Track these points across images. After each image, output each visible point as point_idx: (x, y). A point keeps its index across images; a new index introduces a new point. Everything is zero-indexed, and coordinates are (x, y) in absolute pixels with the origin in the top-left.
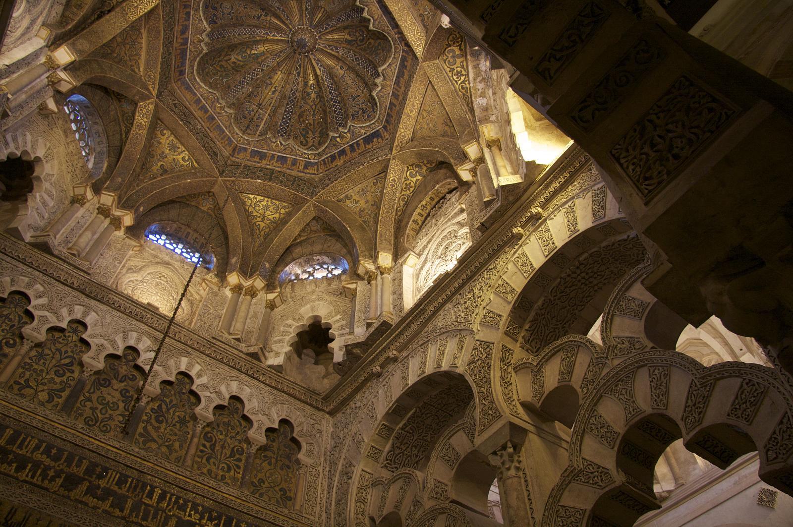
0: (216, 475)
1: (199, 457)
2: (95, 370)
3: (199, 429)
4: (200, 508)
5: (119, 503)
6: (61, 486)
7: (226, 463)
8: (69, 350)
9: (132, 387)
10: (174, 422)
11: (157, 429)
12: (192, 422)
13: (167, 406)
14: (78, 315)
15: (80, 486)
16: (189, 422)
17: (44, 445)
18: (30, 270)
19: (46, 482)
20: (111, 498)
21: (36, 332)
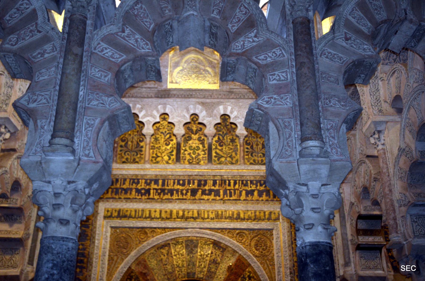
0: (258, 161)
1: (247, 155)
2: (182, 135)
3: (242, 140)
4: (255, 182)
5: (217, 193)
6: (191, 195)
7: (261, 153)
8: (166, 130)
9: (202, 135)
10: (228, 143)
11: (221, 150)
12: (237, 139)
13: (222, 136)
14: (162, 111)
16: (235, 139)
17: (176, 181)
18: (130, 99)
20: (213, 193)
21: (148, 130)
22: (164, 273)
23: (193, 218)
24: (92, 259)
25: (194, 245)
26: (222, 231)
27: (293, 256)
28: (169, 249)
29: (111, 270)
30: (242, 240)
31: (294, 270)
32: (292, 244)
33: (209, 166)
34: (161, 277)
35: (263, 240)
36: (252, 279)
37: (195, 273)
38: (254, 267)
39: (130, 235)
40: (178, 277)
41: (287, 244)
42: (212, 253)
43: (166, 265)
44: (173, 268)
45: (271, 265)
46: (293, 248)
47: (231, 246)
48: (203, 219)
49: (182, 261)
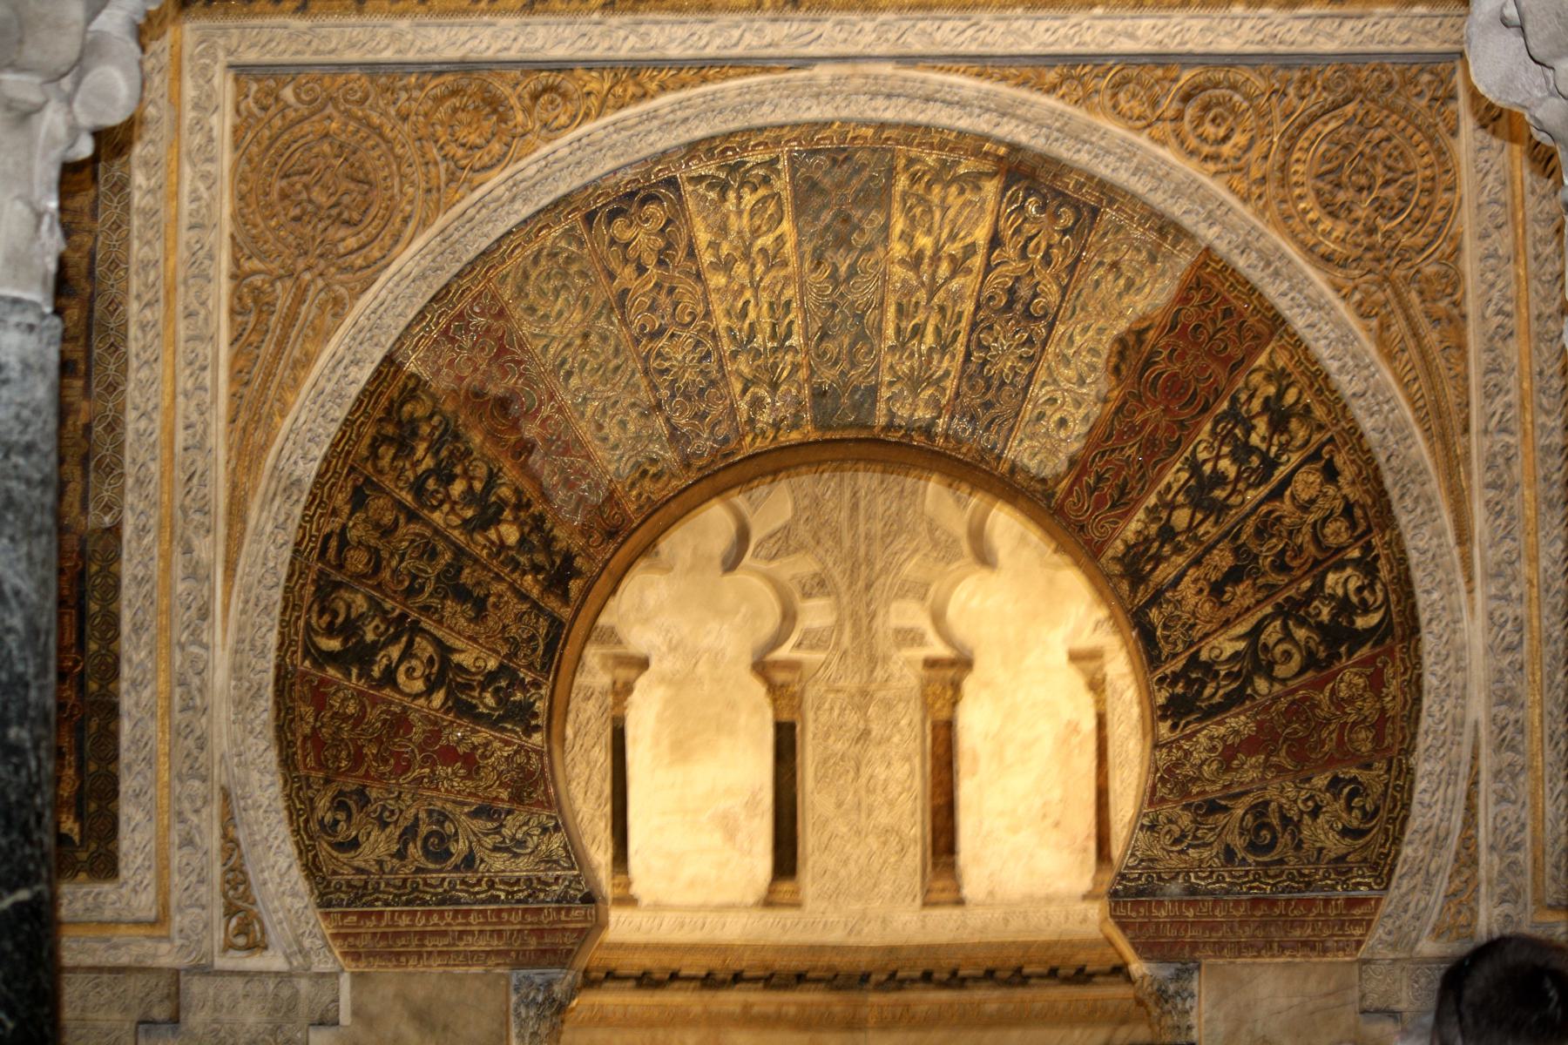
22: (645, 395)
24: (115, 306)
25: (855, 183)
28: (669, 222)
34: (623, 424)
35: (1379, 133)
36: (1294, 424)
37: (873, 391)
39: (376, 119)
40: (751, 421)
42: (995, 241)
43: (656, 334)
44: (708, 355)
47: (1139, 185)
49: (771, 304)
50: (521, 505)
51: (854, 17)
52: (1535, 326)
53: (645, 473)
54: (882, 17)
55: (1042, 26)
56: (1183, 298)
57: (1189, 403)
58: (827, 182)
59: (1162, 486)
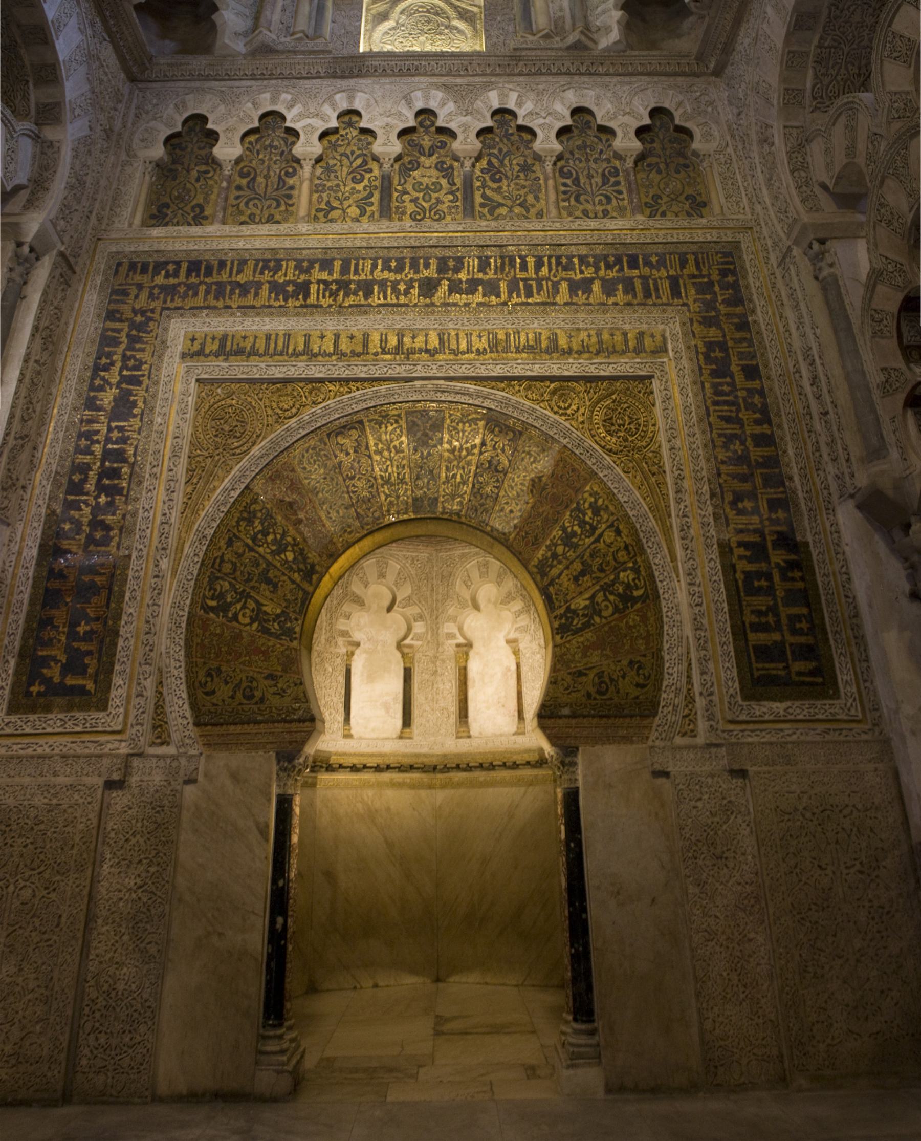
2: (393, 156)
6: (419, 296)
15: (439, 288)
19: (402, 298)
20: (480, 288)
23: (427, 351)
25: (430, 422)
26: (508, 386)
27: (714, 447)
28: (359, 436)
29: (194, 497)
30: (565, 409)
31: (720, 485)
32: (708, 415)
33: (469, 223)
34: (338, 512)
35: (626, 405)
36: (602, 513)
37: (436, 499)
38: (605, 479)
40: (388, 511)
41: (693, 414)
42: (483, 444)
45: (654, 474)
46: (710, 424)
48: (456, 352)
49: (397, 467)
50: (296, 544)
51: (429, 363)
52: (693, 474)
53: (345, 531)
54: (440, 363)
55: (498, 367)
56: (557, 465)
57: (560, 504)
58: (419, 423)
59: (552, 537)
